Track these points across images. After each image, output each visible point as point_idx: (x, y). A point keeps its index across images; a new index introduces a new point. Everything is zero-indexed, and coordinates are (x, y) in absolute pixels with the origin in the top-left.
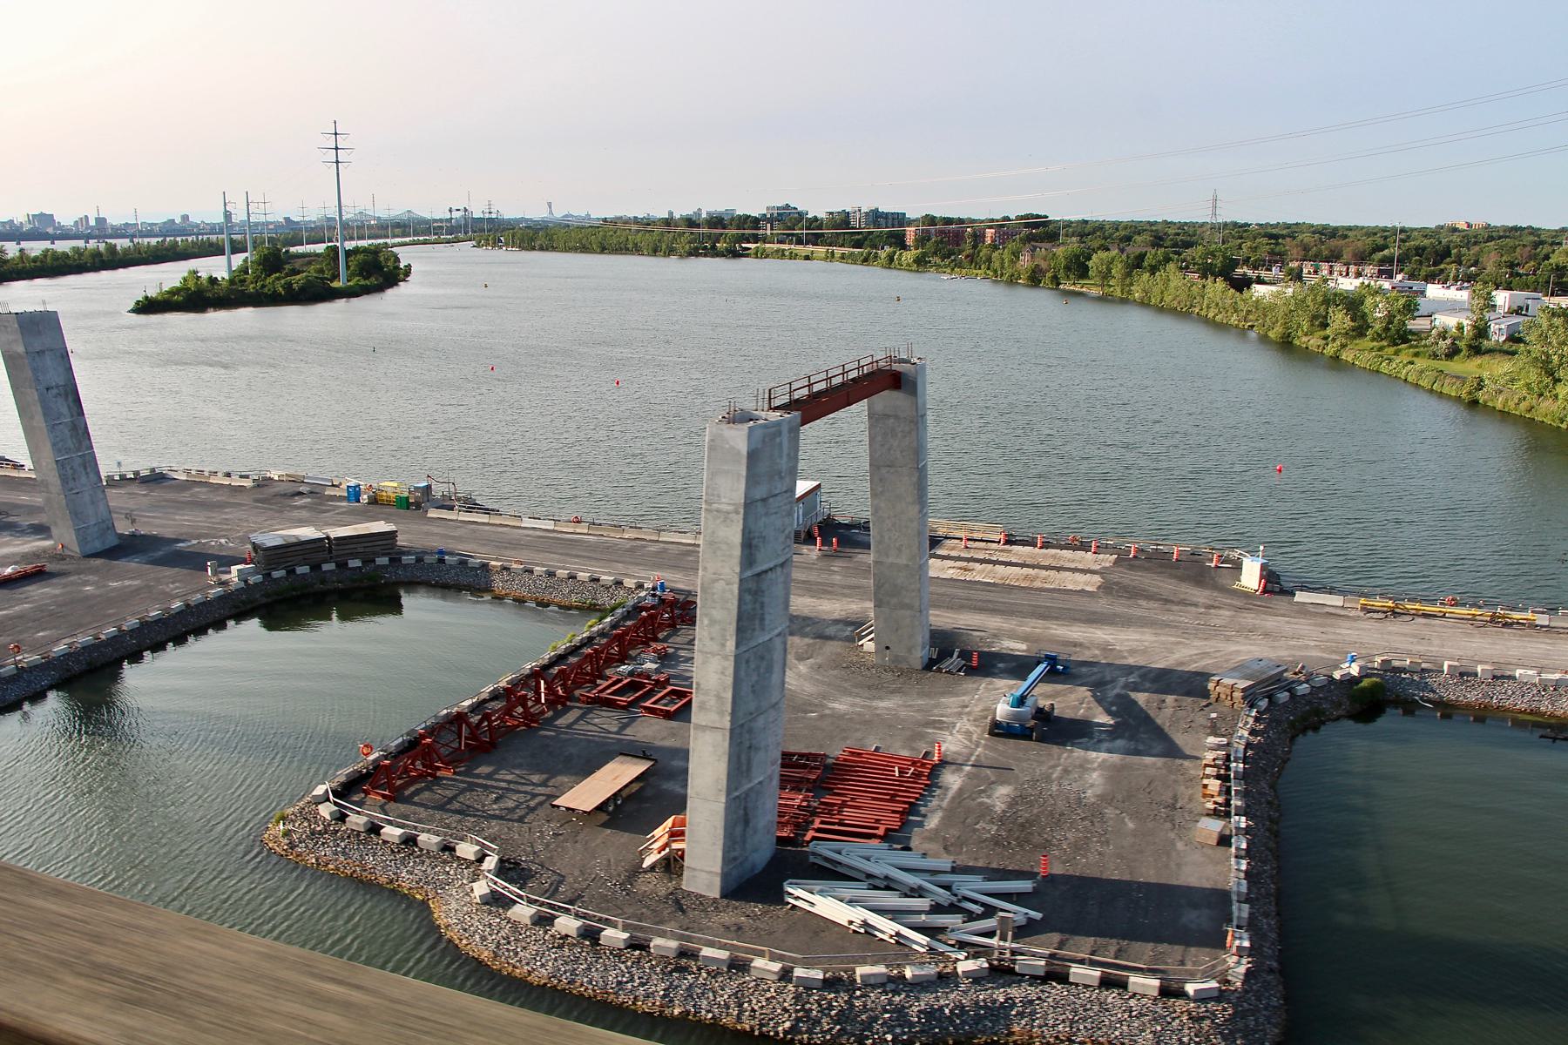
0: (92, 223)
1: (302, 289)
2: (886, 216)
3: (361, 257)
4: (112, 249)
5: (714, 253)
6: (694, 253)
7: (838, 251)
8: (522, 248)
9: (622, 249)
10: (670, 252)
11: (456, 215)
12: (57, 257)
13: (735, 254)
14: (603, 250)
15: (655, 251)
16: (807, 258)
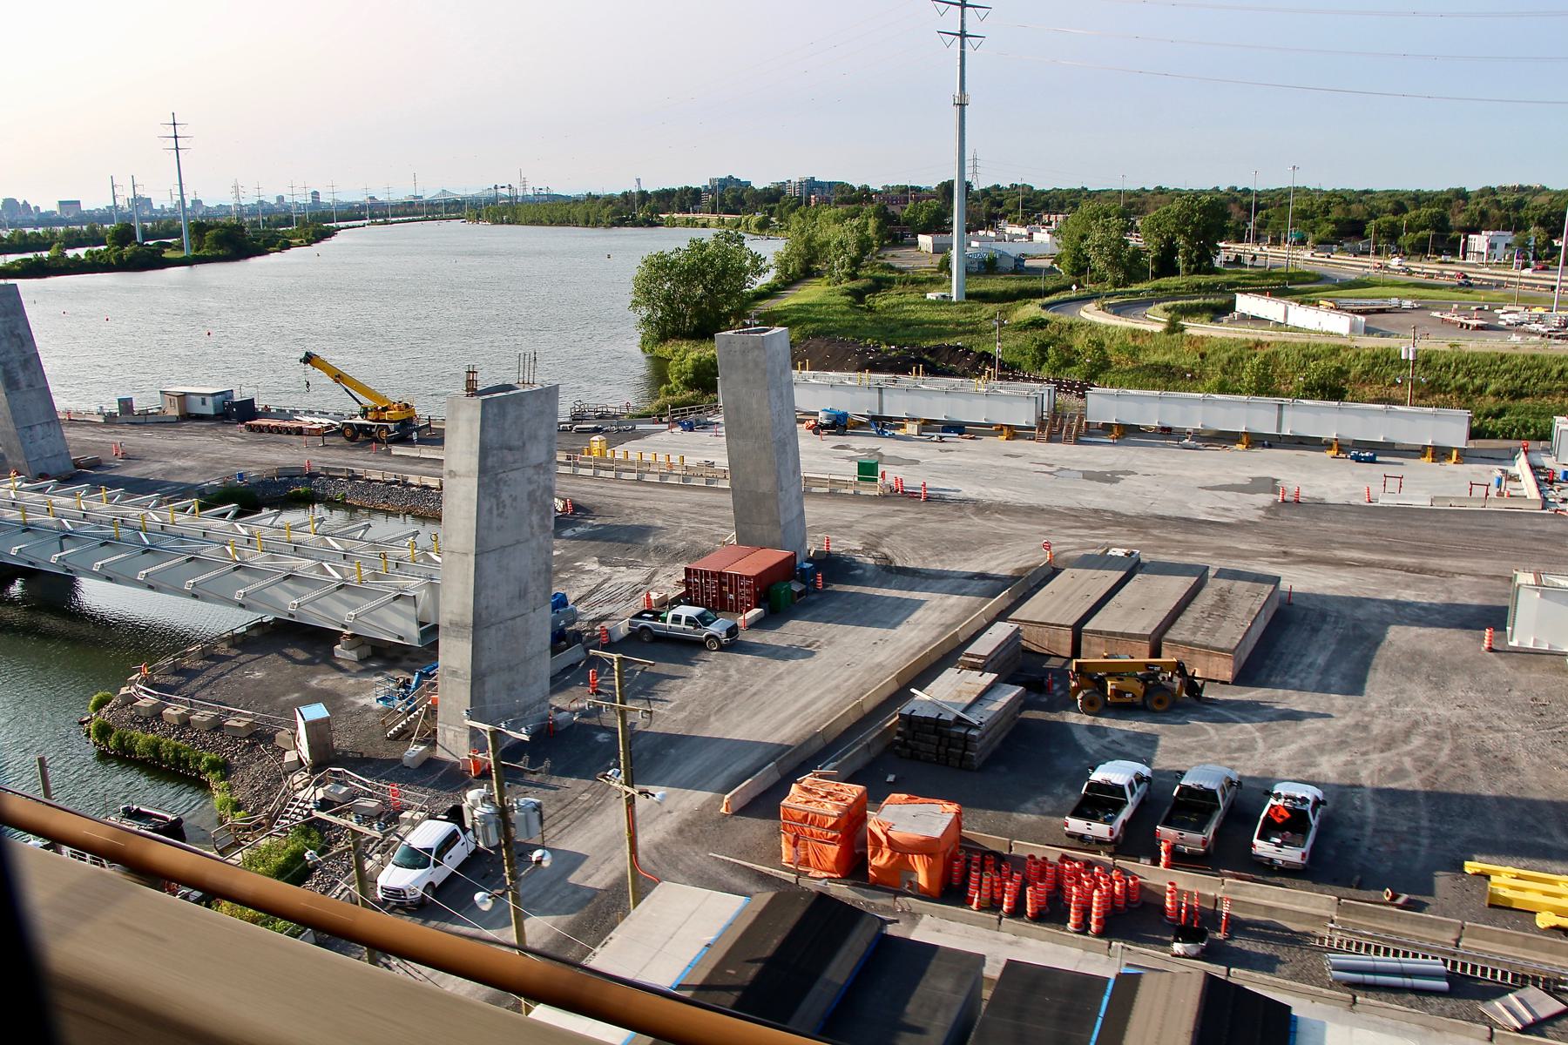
0: (189, 205)
1: (130, 259)
2: (821, 185)
3: (213, 232)
4: (93, 230)
5: (637, 224)
6: (621, 223)
7: (727, 218)
8: (495, 223)
9: (565, 222)
10: (597, 224)
11: (500, 191)
12: (25, 237)
13: (653, 225)
14: (551, 223)
15: (587, 223)
16: (704, 226)
